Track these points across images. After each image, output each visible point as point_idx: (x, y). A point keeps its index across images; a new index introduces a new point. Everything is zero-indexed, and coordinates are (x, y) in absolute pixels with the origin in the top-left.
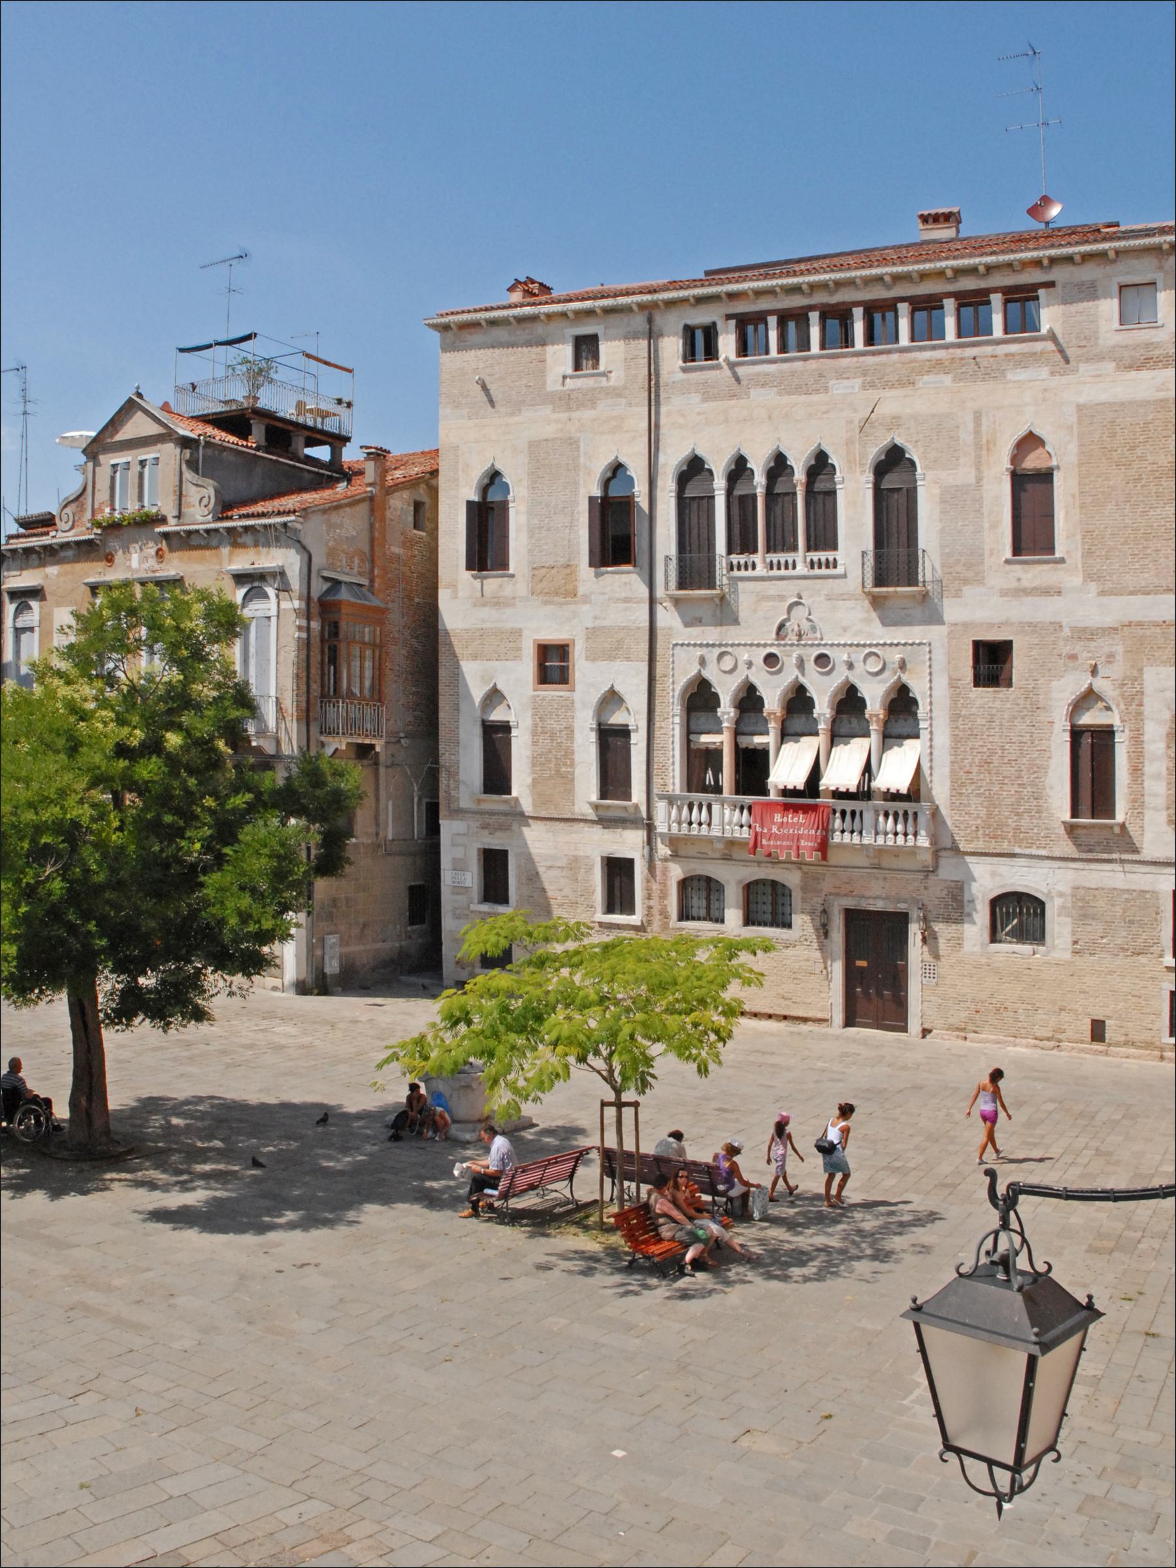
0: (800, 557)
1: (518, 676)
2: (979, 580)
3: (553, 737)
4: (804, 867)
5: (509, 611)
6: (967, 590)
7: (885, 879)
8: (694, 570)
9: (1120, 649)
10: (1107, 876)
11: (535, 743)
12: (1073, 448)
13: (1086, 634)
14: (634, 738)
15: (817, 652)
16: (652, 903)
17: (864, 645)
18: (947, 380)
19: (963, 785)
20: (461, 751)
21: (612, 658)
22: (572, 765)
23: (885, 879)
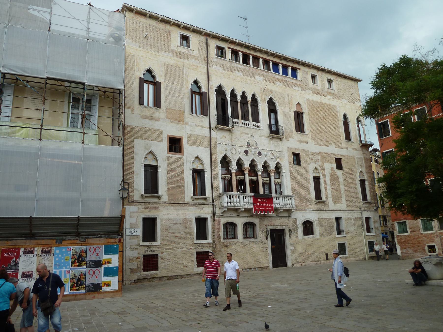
0: (251, 123)
1: (161, 148)
2: (293, 138)
3: (176, 172)
5: (157, 123)
6: (290, 139)
8: (223, 120)
9: (319, 158)
10: (325, 215)
11: (168, 174)
12: (307, 108)
13: (313, 154)
14: (206, 174)
16: (215, 234)
18: (281, 84)
19: (294, 191)
20: (135, 176)
22: (184, 183)
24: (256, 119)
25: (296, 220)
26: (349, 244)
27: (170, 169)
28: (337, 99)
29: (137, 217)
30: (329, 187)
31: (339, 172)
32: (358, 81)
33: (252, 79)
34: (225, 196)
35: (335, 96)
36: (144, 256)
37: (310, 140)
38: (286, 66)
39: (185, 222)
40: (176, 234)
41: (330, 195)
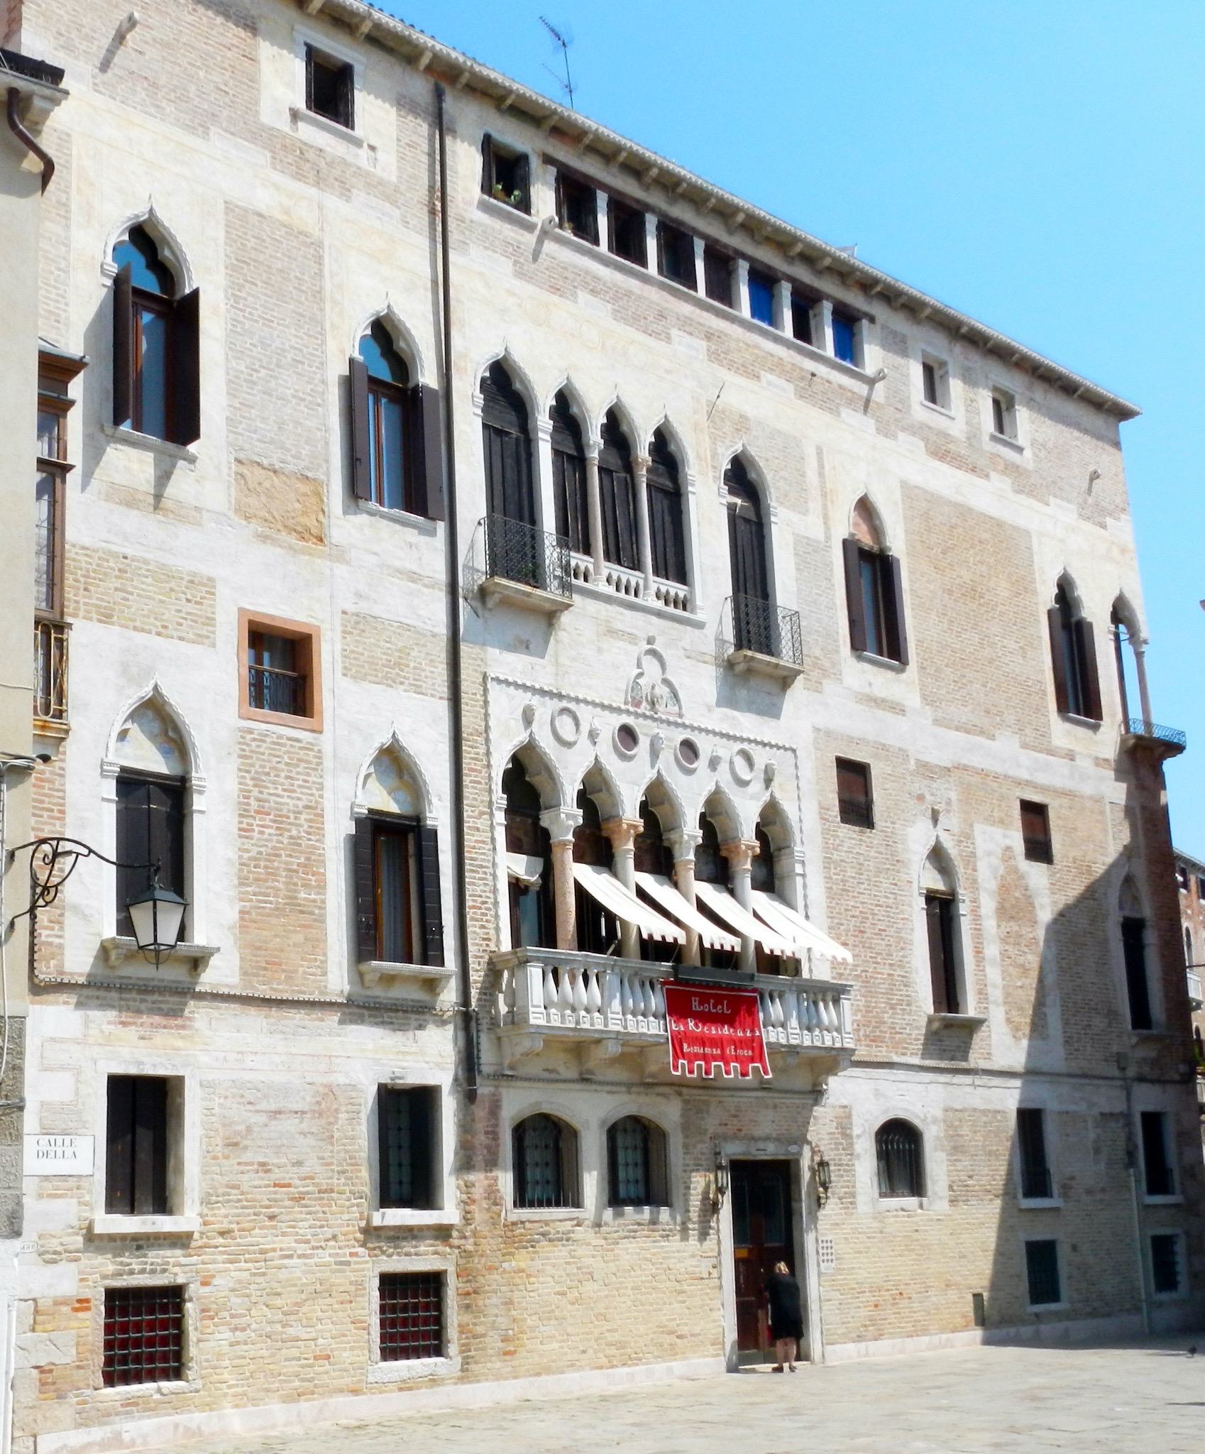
3: (281, 822)
4: (685, 1090)
7: (775, 1107)
8: (515, 552)
9: (953, 796)
11: (245, 832)
13: (927, 770)
15: (681, 735)
17: (735, 738)
21: (390, 681)
23: (775, 1107)
24: (674, 562)
25: (849, 1117)
26: (1074, 1248)
27: (254, 805)
28: (1031, 494)
29: (78, 1072)
30: (992, 950)
31: (1036, 873)
32: (1122, 413)
33: (651, 342)
34: (535, 972)
35: (1024, 483)
36: (111, 1294)
37: (913, 699)
38: (816, 298)
39: (326, 1102)
40: (277, 1175)
41: (996, 994)
